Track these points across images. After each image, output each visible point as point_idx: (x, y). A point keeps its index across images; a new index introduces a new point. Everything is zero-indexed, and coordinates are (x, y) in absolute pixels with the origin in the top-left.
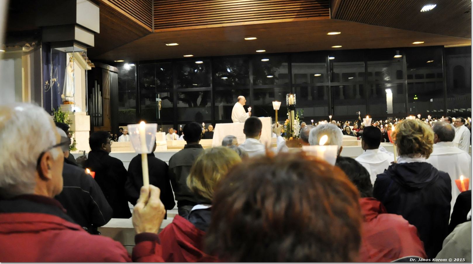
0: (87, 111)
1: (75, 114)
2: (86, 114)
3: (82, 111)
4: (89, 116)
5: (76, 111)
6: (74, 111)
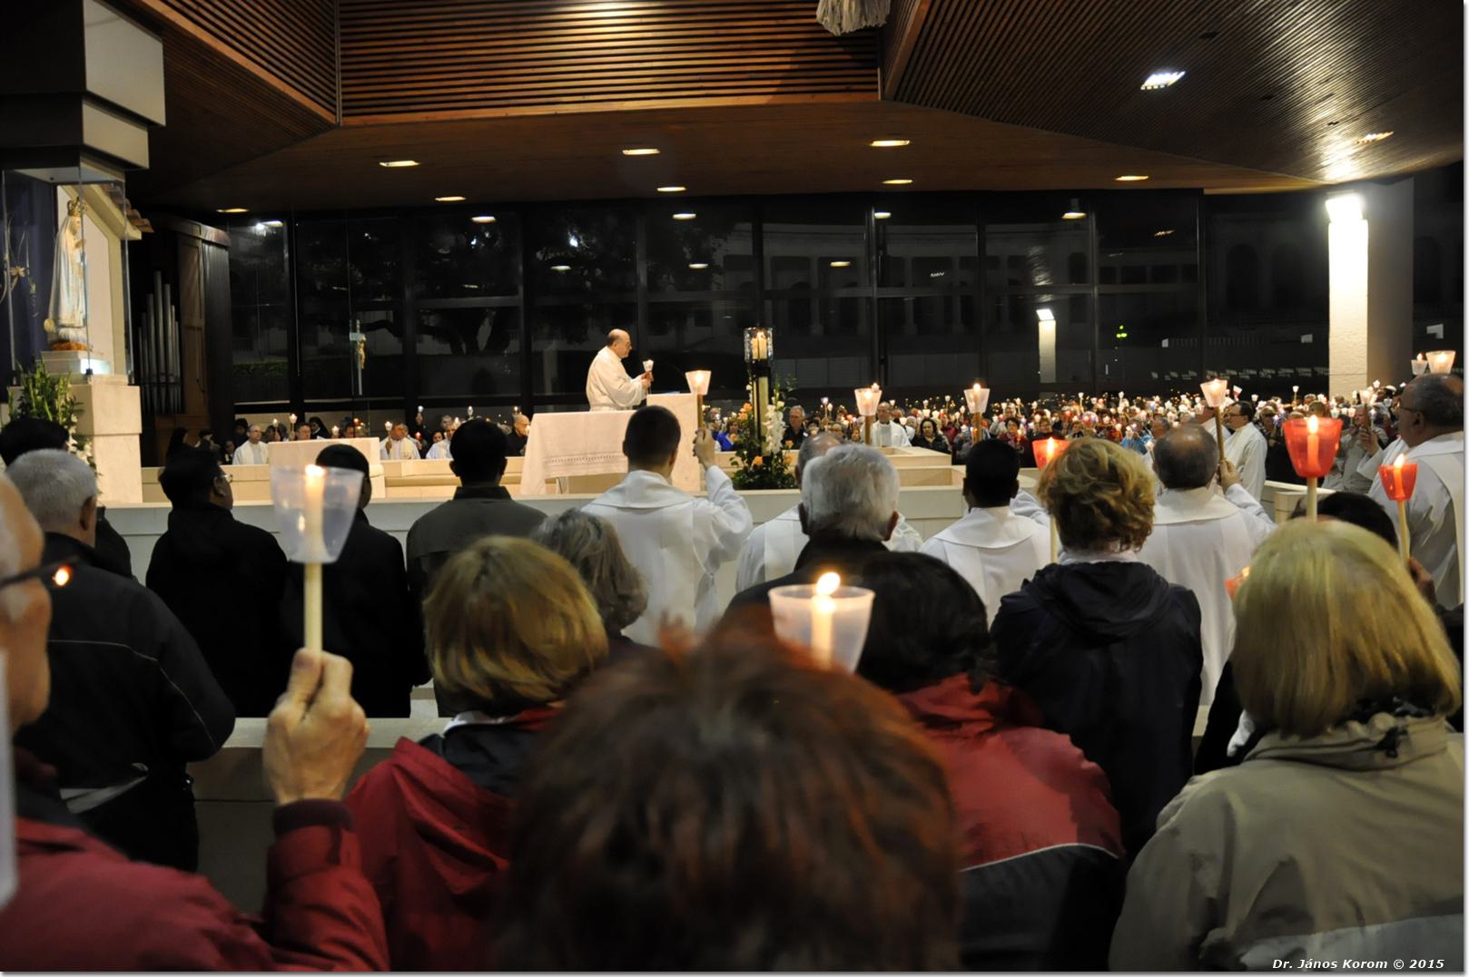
0: (129, 372)
1: (92, 381)
2: (127, 381)
3: (115, 372)
4: (138, 388)
5: (94, 372)
6: (89, 372)
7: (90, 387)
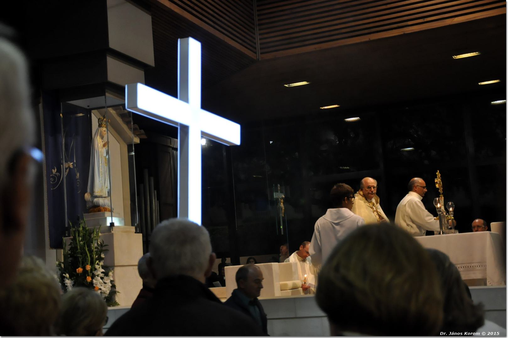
2: (134, 230)
3: (125, 225)
4: (140, 236)
5: (115, 225)
6: (112, 224)
7: (113, 234)
